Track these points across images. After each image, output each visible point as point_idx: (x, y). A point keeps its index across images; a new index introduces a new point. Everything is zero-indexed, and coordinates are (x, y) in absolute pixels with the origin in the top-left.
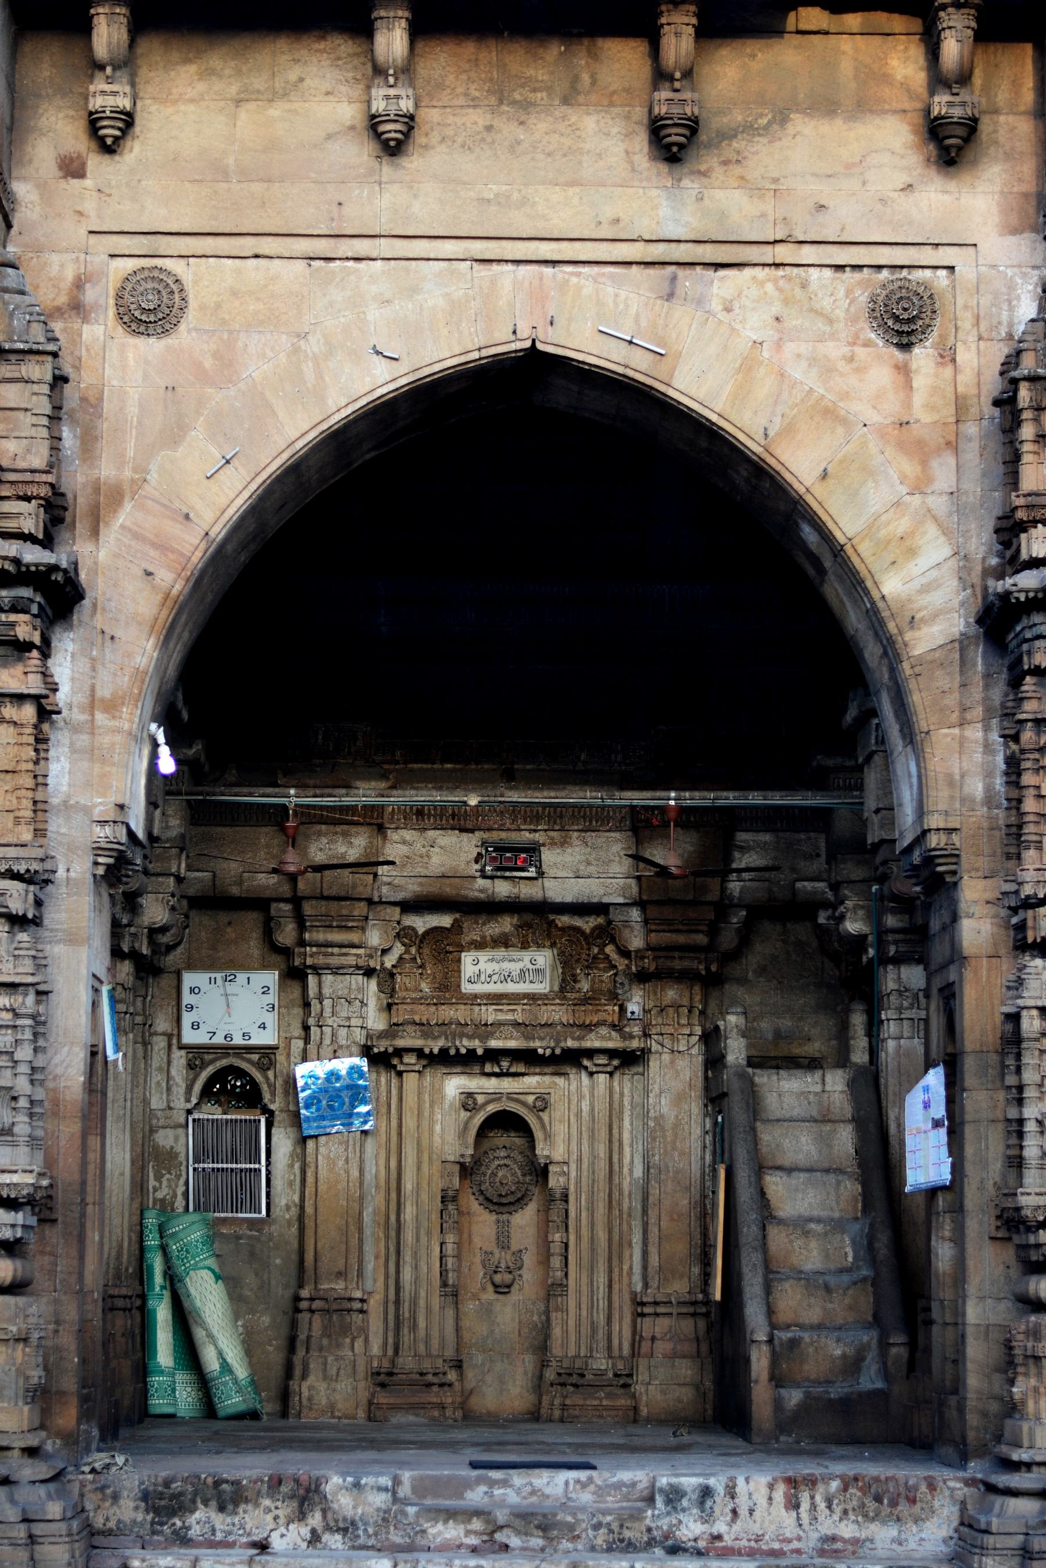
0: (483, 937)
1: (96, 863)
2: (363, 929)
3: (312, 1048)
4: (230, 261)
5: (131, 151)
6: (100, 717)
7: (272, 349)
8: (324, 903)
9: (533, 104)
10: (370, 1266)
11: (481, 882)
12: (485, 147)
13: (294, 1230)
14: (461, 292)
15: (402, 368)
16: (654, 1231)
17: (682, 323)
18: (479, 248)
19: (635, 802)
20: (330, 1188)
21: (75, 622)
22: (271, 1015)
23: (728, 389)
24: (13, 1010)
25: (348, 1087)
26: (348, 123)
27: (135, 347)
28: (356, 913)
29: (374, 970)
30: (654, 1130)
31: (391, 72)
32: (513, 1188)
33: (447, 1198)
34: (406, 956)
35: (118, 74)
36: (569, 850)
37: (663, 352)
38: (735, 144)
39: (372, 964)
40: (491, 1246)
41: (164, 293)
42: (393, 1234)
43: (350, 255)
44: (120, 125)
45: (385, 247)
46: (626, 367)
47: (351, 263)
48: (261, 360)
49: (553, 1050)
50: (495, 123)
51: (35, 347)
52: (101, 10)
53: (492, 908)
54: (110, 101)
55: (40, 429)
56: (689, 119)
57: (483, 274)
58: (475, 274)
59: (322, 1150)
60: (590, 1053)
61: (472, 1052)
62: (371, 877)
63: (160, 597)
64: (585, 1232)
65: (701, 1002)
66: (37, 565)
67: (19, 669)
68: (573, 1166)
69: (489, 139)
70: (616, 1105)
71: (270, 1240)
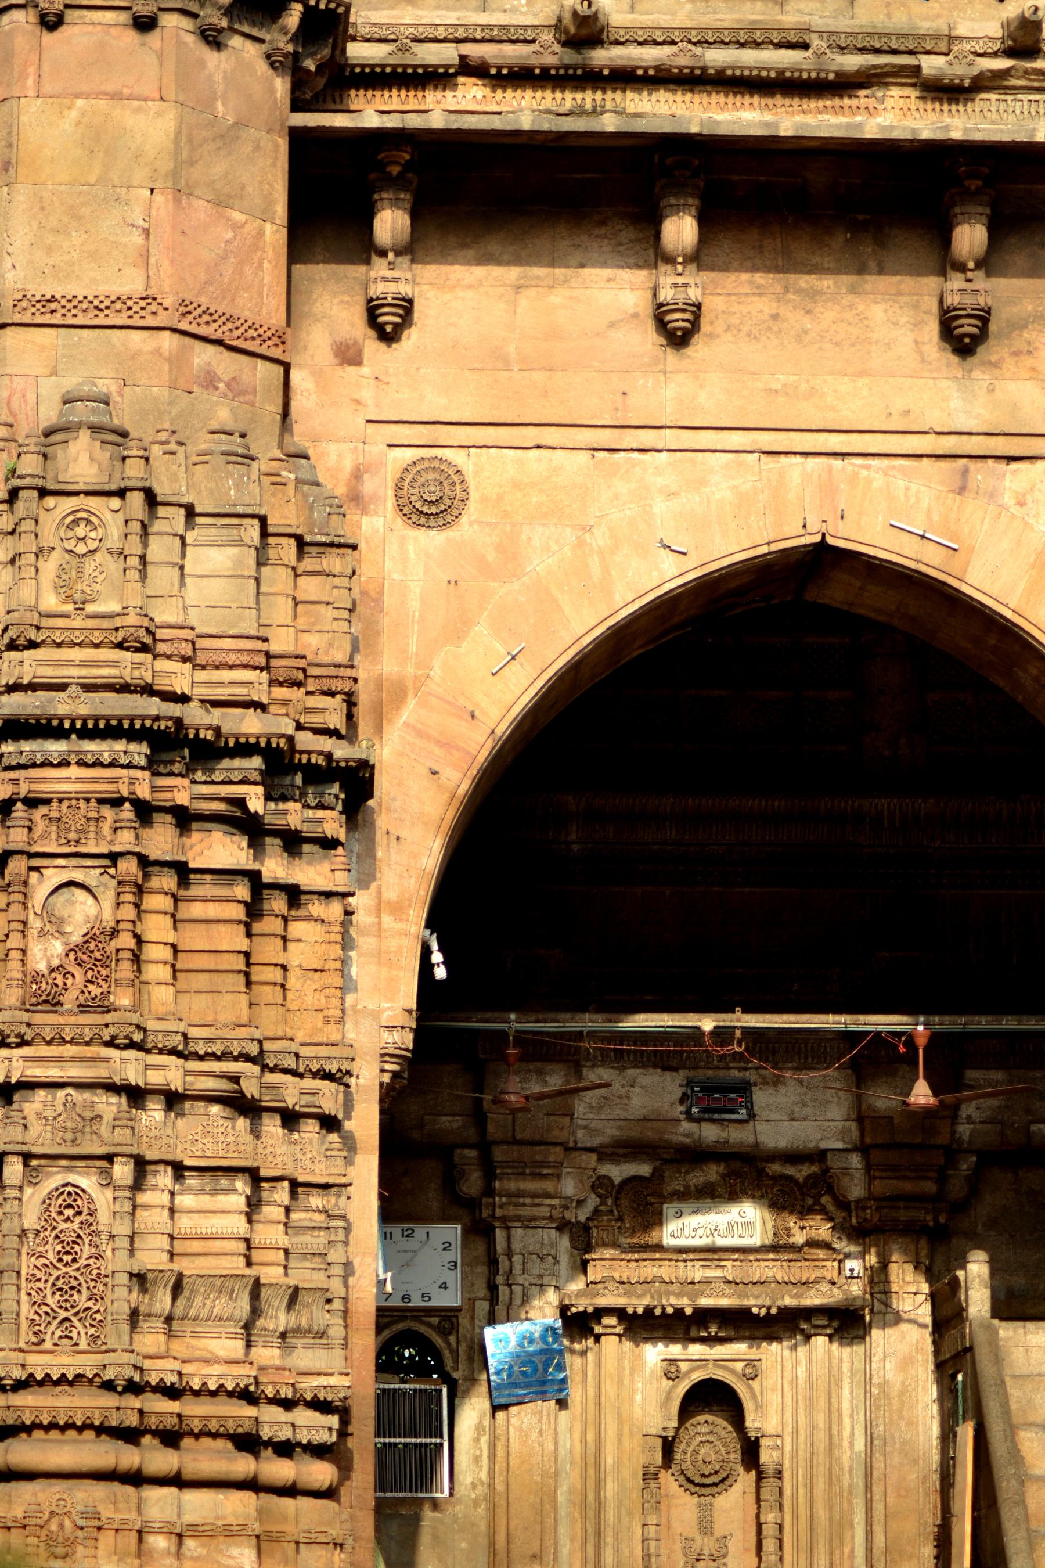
0: (687, 1187)
1: (383, 1071)
2: (559, 1177)
3: (500, 1309)
4: (512, 451)
5: (409, 338)
6: (387, 920)
7: (557, 542)
8: (515, 1148)
9: (821, 293)
10: (565, 1550)
11: (686, 1126)
12: (772, 336)
13: (482, 1510)
14: (749, 485)
15: (690, 562)
16: (878, 1508)
17: (975, 518)
18: (767, 440)
19: (880, 1028)
20: (523, 1463)
21: (360, 822)
22: (452, 1273)
23: (1022, 585)
24: (326, 1212)
25: (542, 1352)
26: (631, 311)
27: (416, 539)
28: (551, 1159)
29: (569, 1222)
30: (878, 1398)
31: (680, 260)
32: (717, 1468)
33: (649, 1476)
34: (602, 1208)
35: (400, 259)
36: (782, 1090)
37: (956, 547)
38: (1026, 335)
39: (569, 1215)
40: (693, 1531)
41: (445, 484)
42: (591, 1514)
43: (635, 446)
44: (401, 312)
45: (670, 439)
46: (918, 561)
47: (636, 454)
48: (545, 552)
49: (769, 1308)
50: (781, 311)
51: (336, 540)
52: (385, 195)
53: (696, 1155)
54: (392, 288)
55: (342, 623)
56: (982, 310)
57: (771, 466)
58: (763, 467)
59: (514, 1421)
60: (808, 1313)
61: (679, 1312)
62: (568, 1119)
63: (446, 797)
64: (803, 1511)
65: (927, 1256)
66: (347, 761)
67: (326, 866)
68: (788, 1440)
69: (775, 329)
70: (835, 1372)
71: (455, 1522)
